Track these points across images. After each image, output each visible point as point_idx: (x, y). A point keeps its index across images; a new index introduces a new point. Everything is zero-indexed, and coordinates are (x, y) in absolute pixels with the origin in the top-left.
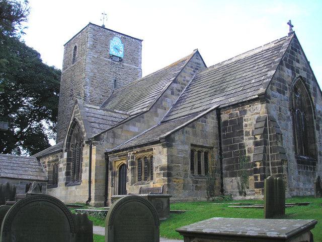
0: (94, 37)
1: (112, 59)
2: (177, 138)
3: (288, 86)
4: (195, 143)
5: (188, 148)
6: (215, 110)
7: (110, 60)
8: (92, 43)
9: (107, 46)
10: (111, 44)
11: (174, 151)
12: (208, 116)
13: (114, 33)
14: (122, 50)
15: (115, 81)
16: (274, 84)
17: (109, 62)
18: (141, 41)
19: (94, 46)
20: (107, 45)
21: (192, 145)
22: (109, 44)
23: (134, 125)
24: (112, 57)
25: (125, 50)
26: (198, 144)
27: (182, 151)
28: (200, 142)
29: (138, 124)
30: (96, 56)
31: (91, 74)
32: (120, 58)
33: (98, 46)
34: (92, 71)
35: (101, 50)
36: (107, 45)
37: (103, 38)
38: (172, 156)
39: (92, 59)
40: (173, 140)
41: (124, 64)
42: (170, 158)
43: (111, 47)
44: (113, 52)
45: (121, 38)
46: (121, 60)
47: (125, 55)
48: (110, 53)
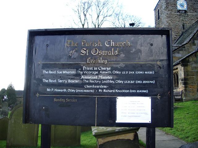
1: (179, 12)
2: (191, 60)
7: (178, 13)
8: (165, 6)
10: (178, 3)
11: (189, 68)
14: (186, 5)
15: (183, 25)
17: (178, 15)
19: (167, 7)
20: (175, 5)
22: (177, 4)
23: (179, 53)
24: (179, 11)
25: (188, 5)
29: (181, 52)
30: (169, 13)
32: (185, 10)
36: (175, 5)
38: (187, 71)
40: (188, 62)
41: (188, 14)
42: (186, 73)
44: (179, 8)
46: (185, 11)
47: (188, 9)
48: (178, 9)
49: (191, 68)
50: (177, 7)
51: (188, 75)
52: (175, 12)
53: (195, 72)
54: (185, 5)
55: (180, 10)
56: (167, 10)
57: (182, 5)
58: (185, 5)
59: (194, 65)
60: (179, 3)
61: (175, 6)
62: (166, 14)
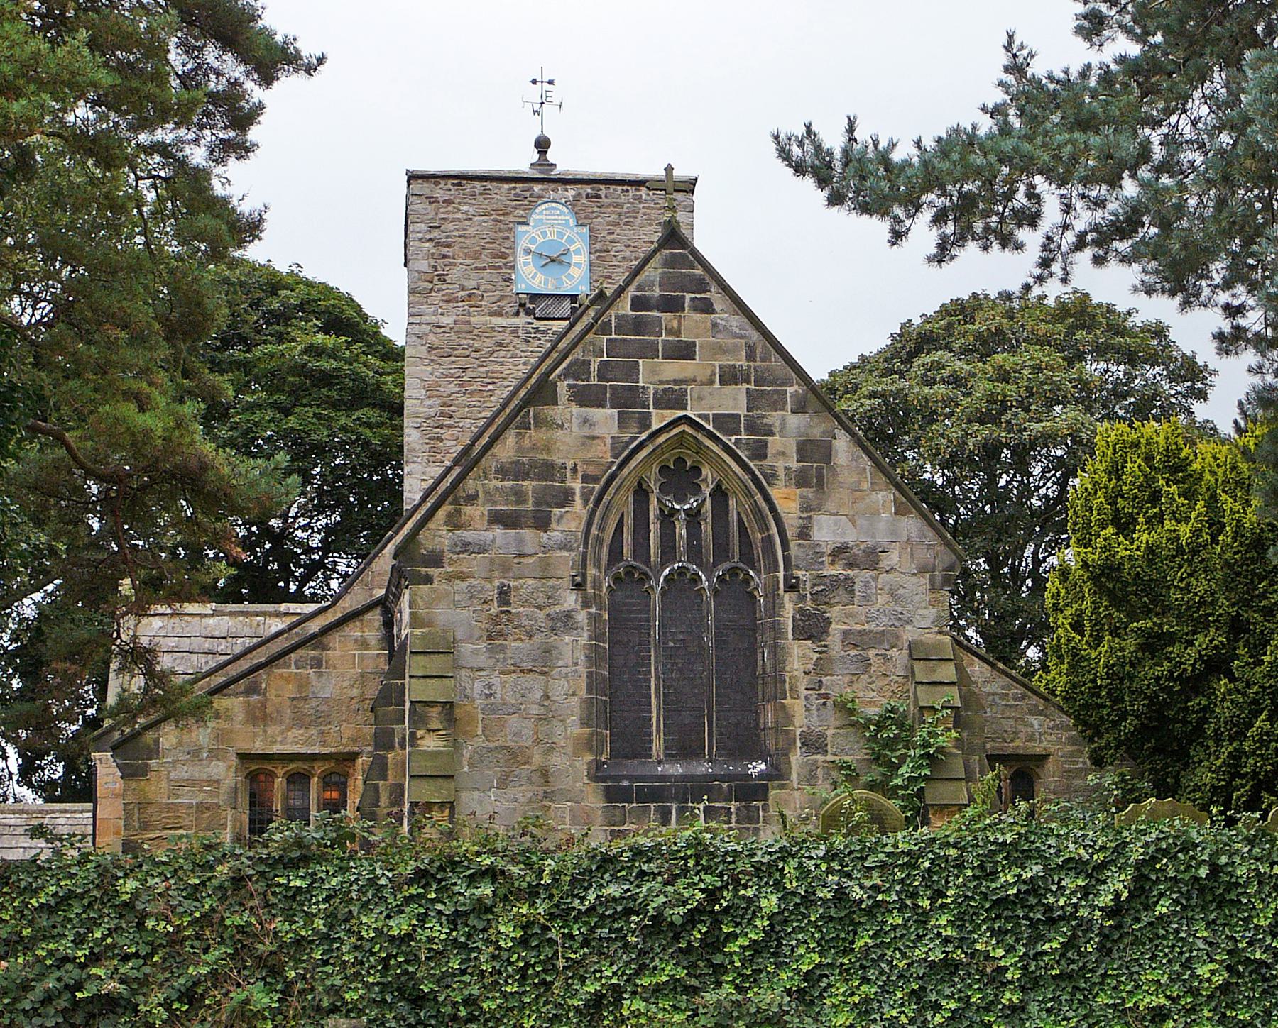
0: (435, 234)
1: (529, 312)
3: (577, 486)
4: (259, 747)
5: (225, 772)
6: (378, 611)
7: (523, 319)
9: (502, 258)
10: (523, 243)
12: (334, 639)
13: (537, 188)
16: (472, 498)
17: (514, 332)
18: (689, 186)
20: (504, 256)
21: (243, 757)
24: (532, 303)
25: (599, 253)
26: (276, 749)
27: (193, 783)
28: (291, 741)
31: (431, 407)
32: (574, 298)
33: (458, 273)
34: (431, 390)
35: (473, 284)
36: (504, 256)
37: (480, 227)
38: (143, 805)
39: (431, 337)
43: (521, 259)
44: (530, 278)
45: (573, 204)
49: (164, 784)
50: (513, 267)
51: (145, 826)
52: (499, 314)
53: (190, 806)
54: (577, 252)
55: (534, 297)
56: (437, 297)
57: (556, 261)
58: (577, 252)
59: (182, 772)
60: (533, 240)
61: (500, 262)
62: (427, 328)
